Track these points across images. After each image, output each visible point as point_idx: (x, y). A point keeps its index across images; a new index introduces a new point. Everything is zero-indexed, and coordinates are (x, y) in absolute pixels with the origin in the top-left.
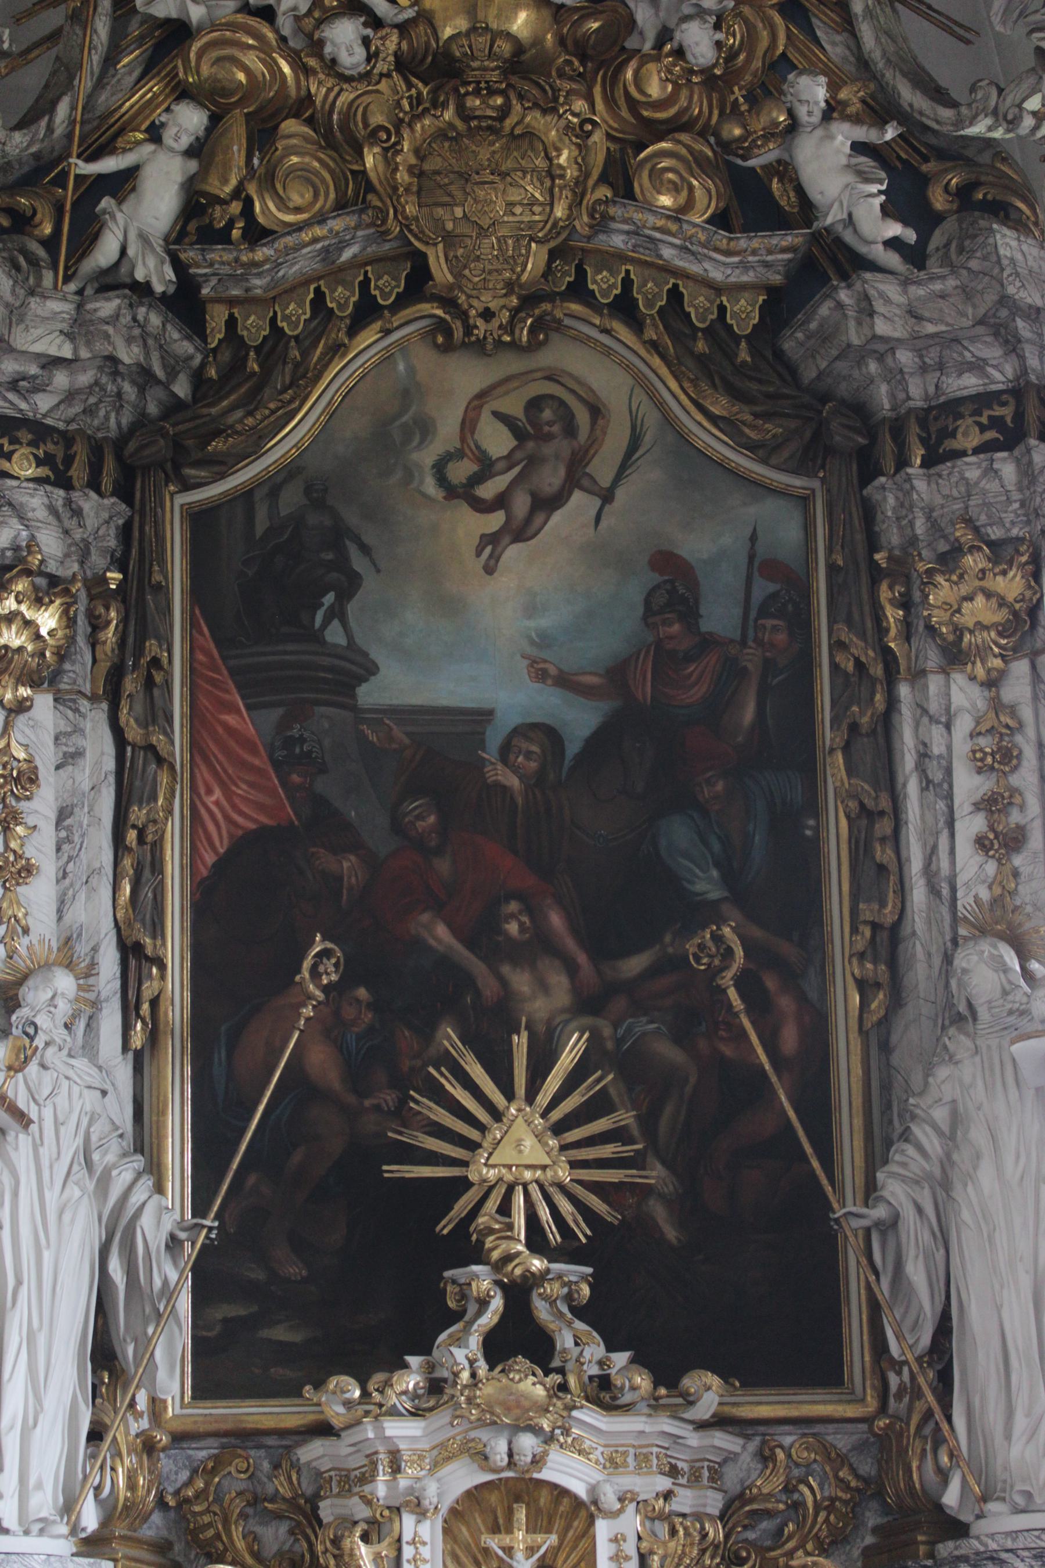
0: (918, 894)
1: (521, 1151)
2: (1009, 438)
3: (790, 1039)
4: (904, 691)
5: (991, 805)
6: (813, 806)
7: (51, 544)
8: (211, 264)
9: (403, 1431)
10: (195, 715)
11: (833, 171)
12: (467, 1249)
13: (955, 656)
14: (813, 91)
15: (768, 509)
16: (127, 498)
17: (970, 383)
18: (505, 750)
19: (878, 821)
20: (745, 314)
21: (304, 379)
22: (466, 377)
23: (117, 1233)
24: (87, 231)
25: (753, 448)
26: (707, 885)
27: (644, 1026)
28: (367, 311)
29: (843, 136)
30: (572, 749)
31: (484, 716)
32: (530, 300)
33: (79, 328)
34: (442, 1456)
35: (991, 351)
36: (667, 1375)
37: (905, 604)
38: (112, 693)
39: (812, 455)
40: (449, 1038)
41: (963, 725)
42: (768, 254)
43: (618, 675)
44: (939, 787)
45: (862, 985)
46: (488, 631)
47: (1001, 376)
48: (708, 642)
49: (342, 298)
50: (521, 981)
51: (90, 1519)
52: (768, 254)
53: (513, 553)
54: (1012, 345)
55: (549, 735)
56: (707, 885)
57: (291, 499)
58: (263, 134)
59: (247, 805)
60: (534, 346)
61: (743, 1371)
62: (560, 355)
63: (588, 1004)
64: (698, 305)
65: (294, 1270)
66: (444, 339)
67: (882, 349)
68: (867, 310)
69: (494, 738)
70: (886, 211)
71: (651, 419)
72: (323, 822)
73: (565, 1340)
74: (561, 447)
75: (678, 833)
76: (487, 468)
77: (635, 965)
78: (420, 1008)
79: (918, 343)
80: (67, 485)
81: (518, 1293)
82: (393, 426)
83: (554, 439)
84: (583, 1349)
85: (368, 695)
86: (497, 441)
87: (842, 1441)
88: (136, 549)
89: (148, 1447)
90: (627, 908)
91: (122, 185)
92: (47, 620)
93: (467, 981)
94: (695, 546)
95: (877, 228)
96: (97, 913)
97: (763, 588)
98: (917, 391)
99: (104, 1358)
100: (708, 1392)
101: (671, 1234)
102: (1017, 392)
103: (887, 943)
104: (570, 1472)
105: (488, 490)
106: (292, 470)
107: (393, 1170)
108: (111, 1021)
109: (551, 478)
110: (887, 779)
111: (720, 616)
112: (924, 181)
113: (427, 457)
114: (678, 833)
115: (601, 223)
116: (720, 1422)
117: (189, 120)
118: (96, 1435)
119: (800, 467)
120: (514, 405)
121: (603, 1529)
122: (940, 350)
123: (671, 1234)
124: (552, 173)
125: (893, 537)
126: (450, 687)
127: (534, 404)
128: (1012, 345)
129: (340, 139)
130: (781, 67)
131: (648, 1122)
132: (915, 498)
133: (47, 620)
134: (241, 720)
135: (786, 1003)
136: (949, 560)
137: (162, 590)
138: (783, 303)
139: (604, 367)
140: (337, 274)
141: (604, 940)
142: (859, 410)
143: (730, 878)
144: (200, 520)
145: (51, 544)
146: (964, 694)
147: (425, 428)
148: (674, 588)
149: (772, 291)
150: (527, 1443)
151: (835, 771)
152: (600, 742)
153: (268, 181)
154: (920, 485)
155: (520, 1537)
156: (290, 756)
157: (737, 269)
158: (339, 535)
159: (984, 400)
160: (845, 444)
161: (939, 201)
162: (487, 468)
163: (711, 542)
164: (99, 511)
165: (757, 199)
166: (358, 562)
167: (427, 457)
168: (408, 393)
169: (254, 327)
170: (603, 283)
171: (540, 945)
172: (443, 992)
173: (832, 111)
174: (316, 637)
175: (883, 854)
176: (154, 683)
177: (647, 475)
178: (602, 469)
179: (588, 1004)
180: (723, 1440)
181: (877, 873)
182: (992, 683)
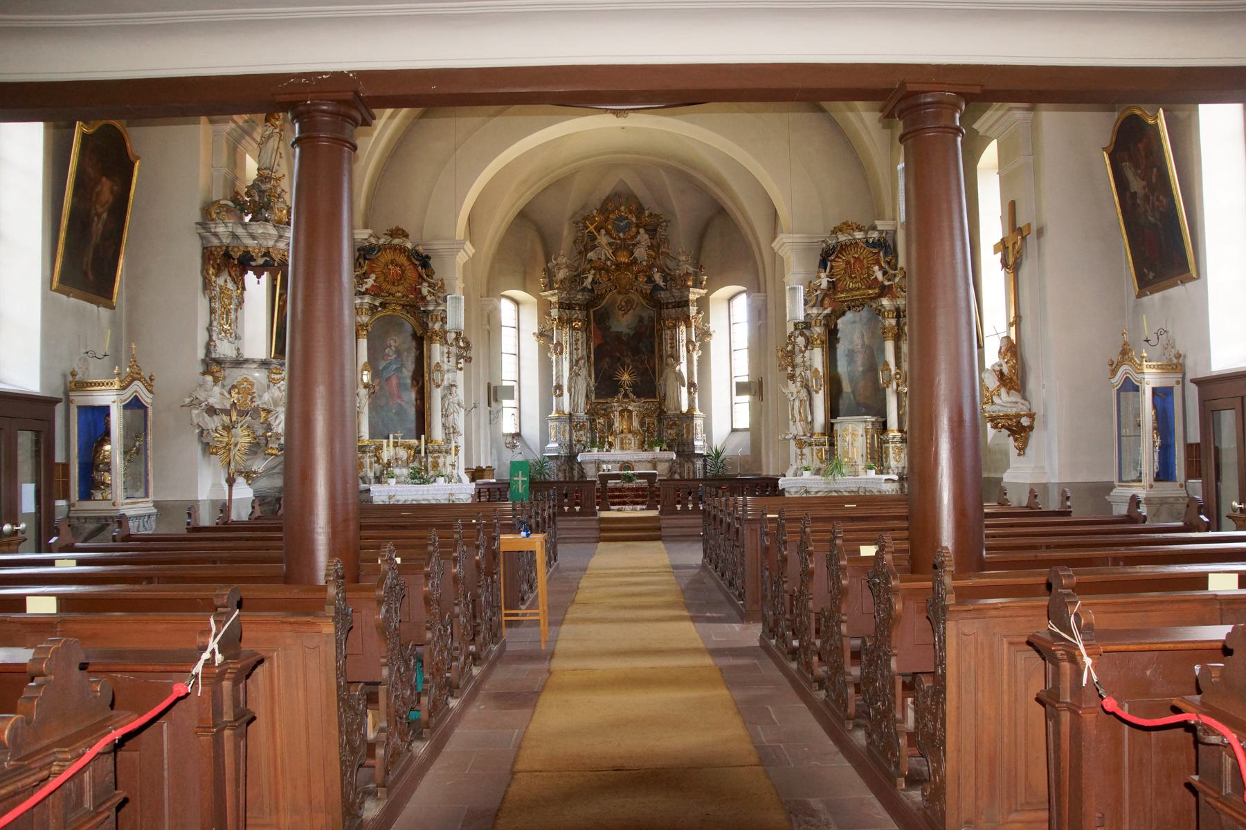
11: (657, 277)
19: (661, 344)
22: (621, 297)
23: (588, 385)
46: (623, 323)
66: (619, 293)
83: (629, 304)
84: (631, 395)
88: (588, 316)
90: (636, 351)
95: (662, 284)
103: (661, 356)
111: (646, 322)
126: (620, 329)
129: (607, 271)
130: (653, 265)
132: (665, 312)
138: (652, 291)
139: (635, 297)
157: (648, 288)
160: (659, 305)
163: (645, 314)
165: (650, 280)
181: (660, 350)
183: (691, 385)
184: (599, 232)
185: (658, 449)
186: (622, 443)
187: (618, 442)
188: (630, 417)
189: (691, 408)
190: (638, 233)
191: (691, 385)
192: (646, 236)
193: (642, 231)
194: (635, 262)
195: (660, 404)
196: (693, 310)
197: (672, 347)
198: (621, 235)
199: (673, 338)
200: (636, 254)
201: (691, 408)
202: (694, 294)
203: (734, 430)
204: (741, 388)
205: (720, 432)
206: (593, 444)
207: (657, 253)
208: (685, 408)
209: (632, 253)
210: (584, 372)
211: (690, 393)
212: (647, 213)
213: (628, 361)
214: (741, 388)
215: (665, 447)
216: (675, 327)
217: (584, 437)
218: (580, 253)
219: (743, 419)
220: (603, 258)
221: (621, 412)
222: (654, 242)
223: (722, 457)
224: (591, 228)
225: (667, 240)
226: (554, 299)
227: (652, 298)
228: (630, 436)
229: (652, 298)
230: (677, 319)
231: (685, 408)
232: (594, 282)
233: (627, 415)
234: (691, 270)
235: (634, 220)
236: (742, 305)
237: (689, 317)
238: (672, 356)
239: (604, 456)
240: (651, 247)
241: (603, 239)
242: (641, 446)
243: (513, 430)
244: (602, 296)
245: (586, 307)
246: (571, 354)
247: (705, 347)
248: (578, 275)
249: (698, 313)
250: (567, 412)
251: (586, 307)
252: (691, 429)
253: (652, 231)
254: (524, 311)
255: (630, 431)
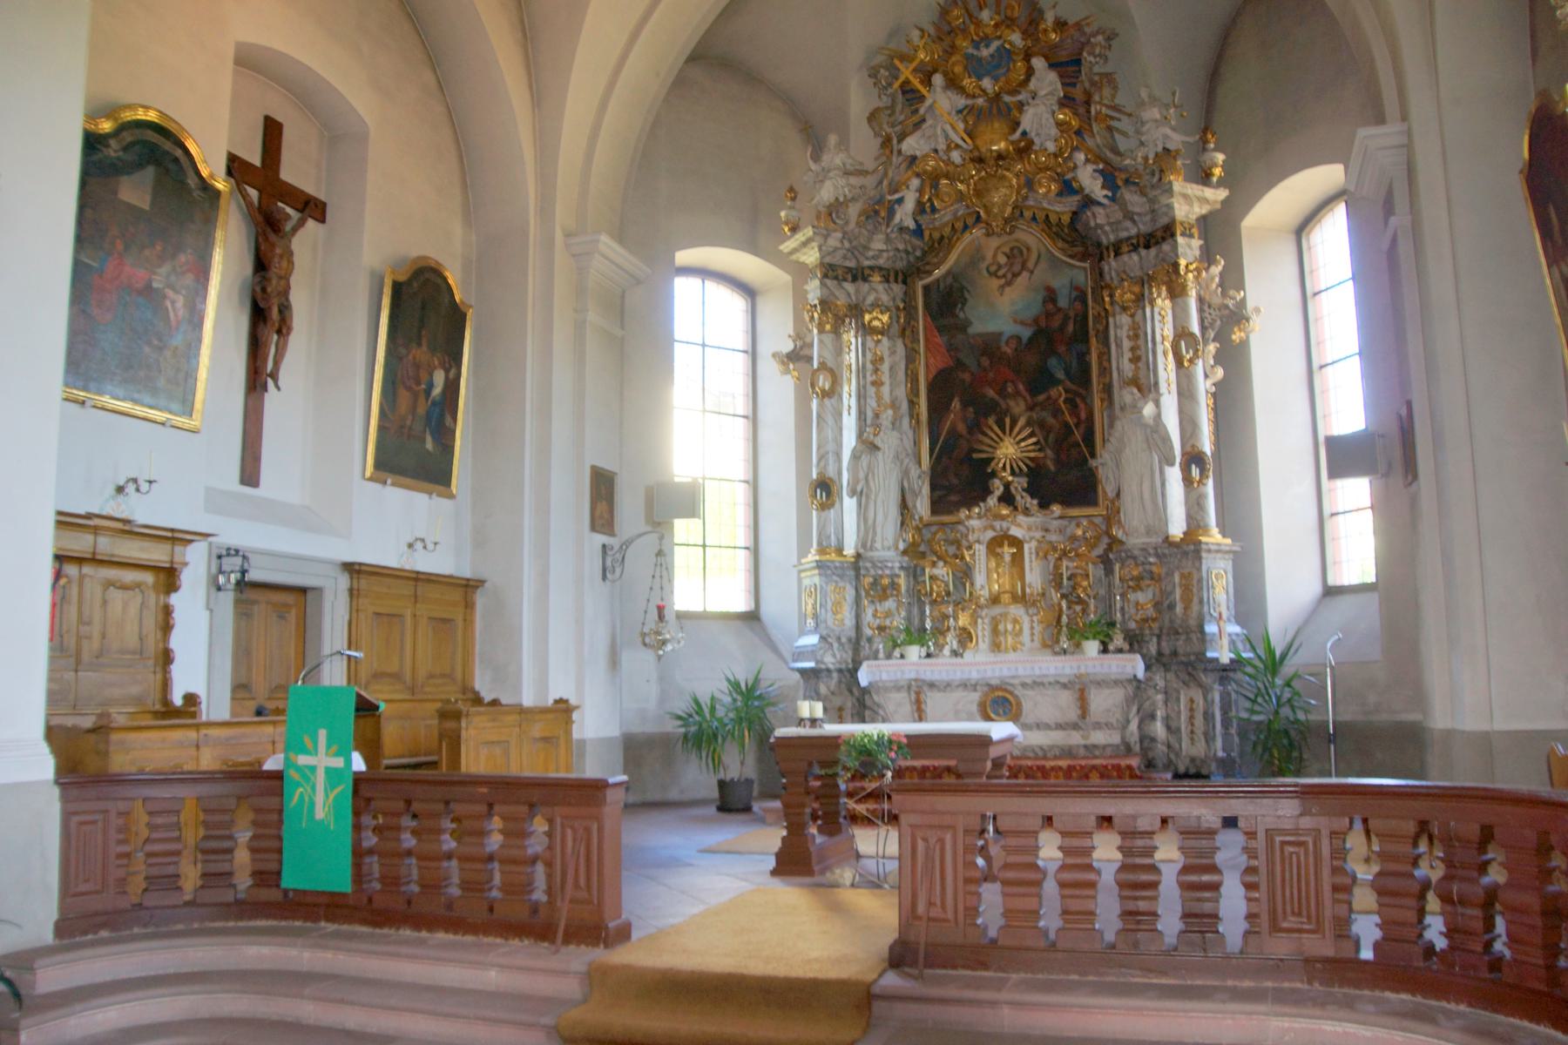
0: (1115, 375)
1: (1008, 450)
2: (1135, 248)
3: (1083, 416)
4: (1111, 320)
5: (1132, 349)
6: (1088, 352)
7: (885, 298)
8: (924, 220)
9: (974, 523)
10: (927, 340)
11: (1089, 179)
12: (994, 474)
13: (1124, 309)
14: (1080, 157)
15: (1076, 271)
16: (904, 282)
17: (1124, 234)
18: (1007, 343)
19: (1105, 355)
20: (1066, 219)
21: (951, 247)
22: (994, 242)
24: (891, 213)
25: (1071, 257)
26: (1060, 375)
27: (1044, 414)
28: (966, 227)
29: (1090, 168)
30: (1025, 340)
31: (1000, 334)
32: (1007, 221)
33: (888, 240)
34: (986, 528)
35: (1128, 224)
36: (1044, 505)
37: (1111, 296)
38: (903, 334)
39: (1083, 257)
40: (991, 421)
41: (1126, 328)
42: (1072, 202)
43: (1036, 321)
44: (1119, 346)
45: (1102, 400)
46: (1002, 311)
47: (1134, 231)
48: (1060, 310)
49: (959, 225)
50: (1012, 403)
51: (902, 546)
52: (1072, 202)
53: (1007, 289)
54: (1134, 222)
55: (1019, 338)
56: (1060, 375)
57: (949, 280)
58: (935, 185)
59: (941, 361)
60: (1011, 233)
61: (1067, 502)
62: (1019, 235)
63: (1031, 408)
64: (1053, 219)
65: (955, 481)
67: (1098, 226)
68: (1094, 216)
69: (1004, 338)
70: (1103, 187)
71: (1043, 249)
72: (960, 365)
73: (1018, 498)
74: (1019, 260)
75: (1053, 362)
76: (1000, 267)
77: (1041, 398)
78: (985, 412)
79: (1110, 224)
80: (888, 281)
81: (1007, 486)
82: (975, 257)
83: (1017, 258)
85: (971, 331)
86: (1002, 259)
87: (1098, 520)
88: (908, 298)
89: (918, 529)
90: (1040, 382)
91: (900, 201)
92: (885, 318)
93: (997, 404)
94: (1055, 284)
96: (902, 392)
97: (1074, 294)
98: (1112, 238)
99: (904, 505)
100: (1056, 509)
101: (1052, 468)
102: (1138, 236)
103: (1108, 389)
104: (1015, 532)
105: (1000, 273)
106: (949, 273)
107: (975, 456)
108: (906, 421)
109: (1017, 268)
110: (1106, 344)
111: (1063, 302)
112: (1115, 178)
113: (983, 266)
114: (1053, 362)
115: (1026, 198)
116: (1061, 517)
117: (915, 182)
118: (902, 524)
119: (1082, 260)
120: (1007, 250)
121: (1026, 546)
122: (1115, 225)
123: (1052, 468)
124: (1011, 186)
125: (1107, 278)
126: (991, 327)
127: (1012, 249)
128: (1134, 222)
131: (1046, 440)
132: (1111, 266)
133: (885, 318)
134: (939, 340)
135: (1082, 406)
136: (1121, 286)
137: (916, 308)
139: (1031, 237)
140: (957, 219)
141: (1034, 390)
142: (1099, 245)
143: (1067, 373)
144: (926, 289)
145: (885, 298)
146: (1124, 319)
147: (983, 258)
148: (1051, 296)
149: (1075, 213)
150: (1005, 525)
151: (1093, 341)
152: (1031, 339)
153: (937, 196)
154: (1113, 264)
155: (1006, 549)
156: (951, 348)
158: (962, 289)
159: (1129, 238)
161: (1120, 183)
162: (1000, 267)
163: (1060, 282)
164: (898, 289)
166: (967, 295)
167: (983, 266)
168: (979, 249)
169: (936, 235)
170: (1028, 214)
171: (1017, 393)
172: (989, 408)
173: (1087, 161)
174: (955, 316)
175: (1105, 364)
176: (914, 332)
177: (1043, 265)
178: (1030, 264)
179: (1031, 408)
180: (1065, 522)
181: (1105, 371)
182: (1132, 316)
183: (1193, 458)
184: (927, 82)
185: (1092, 647)
186: (995, 632)
187: (982, 631)
188: (1018, 559)
189: (1195, 525)
190: (1030, 72)
191: (1193, 458)
192: (1052, 76)
193: (1038, 63)
194: (1024, 149)
195: (1109, 520)
196: (1188, 249)
197: (1135, 359)
198: (987, 83)
199: (1137, 333)
200: (1027, 121)
201: (1195, 525)
202: (1189, 201)
203: (1331, 592)
204: (1342, 457)
205: (1288, 591)
206: (917, 634)
207: (1087, 119)
208: (1177, 528)
209: (1018, 124)
210: (890, 441)
211: (1187, 480)
212: (1050, 17)
213: (1018, 407)
214: (1342, 457)
215: (1118, 641)
216: (1140, 299)
217: (894, 612)
218: (887, 142)
219: (1357, 557)
220: (942, 147)
221: (994, 545)
222: (1078, 93)
223: (1287, 669)
224: (906, 72)
225: (1109, 78)
226: (811, 257)
227: (1077, 237)
228: (1017, 611)
229: (1077, 237)
230: (1145, 281)
231: (1177, 527)
232: (920, 208)
233: (1009, 548)
234: (1176, 140)
235: (1016, 38)
236: (1333, 239)
237: (1176, 265)
238: (1135, 382)
239: (944, 667)
240: (1066, 102)
241: (942, 101)
242: (1050, 644)
243: (739, 602)
244: (940, 245)
245: (904, 276)
246: (861, 397)
247: (1234, 359)
248: (880, 202)
249: (1207, 257)
250: (849, 551)
251: (904, 276)
252: (1193, 587)
253: (1068, 67)
254: (766, 307)
255: (1021, 599)
